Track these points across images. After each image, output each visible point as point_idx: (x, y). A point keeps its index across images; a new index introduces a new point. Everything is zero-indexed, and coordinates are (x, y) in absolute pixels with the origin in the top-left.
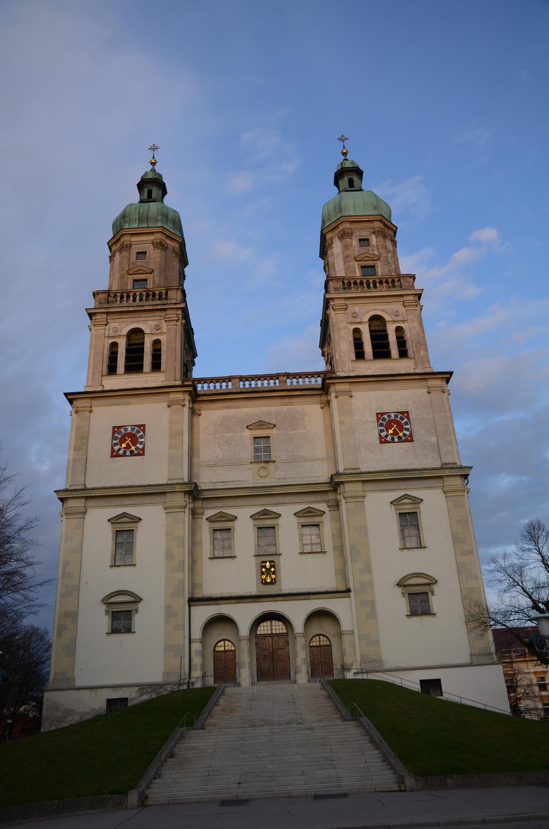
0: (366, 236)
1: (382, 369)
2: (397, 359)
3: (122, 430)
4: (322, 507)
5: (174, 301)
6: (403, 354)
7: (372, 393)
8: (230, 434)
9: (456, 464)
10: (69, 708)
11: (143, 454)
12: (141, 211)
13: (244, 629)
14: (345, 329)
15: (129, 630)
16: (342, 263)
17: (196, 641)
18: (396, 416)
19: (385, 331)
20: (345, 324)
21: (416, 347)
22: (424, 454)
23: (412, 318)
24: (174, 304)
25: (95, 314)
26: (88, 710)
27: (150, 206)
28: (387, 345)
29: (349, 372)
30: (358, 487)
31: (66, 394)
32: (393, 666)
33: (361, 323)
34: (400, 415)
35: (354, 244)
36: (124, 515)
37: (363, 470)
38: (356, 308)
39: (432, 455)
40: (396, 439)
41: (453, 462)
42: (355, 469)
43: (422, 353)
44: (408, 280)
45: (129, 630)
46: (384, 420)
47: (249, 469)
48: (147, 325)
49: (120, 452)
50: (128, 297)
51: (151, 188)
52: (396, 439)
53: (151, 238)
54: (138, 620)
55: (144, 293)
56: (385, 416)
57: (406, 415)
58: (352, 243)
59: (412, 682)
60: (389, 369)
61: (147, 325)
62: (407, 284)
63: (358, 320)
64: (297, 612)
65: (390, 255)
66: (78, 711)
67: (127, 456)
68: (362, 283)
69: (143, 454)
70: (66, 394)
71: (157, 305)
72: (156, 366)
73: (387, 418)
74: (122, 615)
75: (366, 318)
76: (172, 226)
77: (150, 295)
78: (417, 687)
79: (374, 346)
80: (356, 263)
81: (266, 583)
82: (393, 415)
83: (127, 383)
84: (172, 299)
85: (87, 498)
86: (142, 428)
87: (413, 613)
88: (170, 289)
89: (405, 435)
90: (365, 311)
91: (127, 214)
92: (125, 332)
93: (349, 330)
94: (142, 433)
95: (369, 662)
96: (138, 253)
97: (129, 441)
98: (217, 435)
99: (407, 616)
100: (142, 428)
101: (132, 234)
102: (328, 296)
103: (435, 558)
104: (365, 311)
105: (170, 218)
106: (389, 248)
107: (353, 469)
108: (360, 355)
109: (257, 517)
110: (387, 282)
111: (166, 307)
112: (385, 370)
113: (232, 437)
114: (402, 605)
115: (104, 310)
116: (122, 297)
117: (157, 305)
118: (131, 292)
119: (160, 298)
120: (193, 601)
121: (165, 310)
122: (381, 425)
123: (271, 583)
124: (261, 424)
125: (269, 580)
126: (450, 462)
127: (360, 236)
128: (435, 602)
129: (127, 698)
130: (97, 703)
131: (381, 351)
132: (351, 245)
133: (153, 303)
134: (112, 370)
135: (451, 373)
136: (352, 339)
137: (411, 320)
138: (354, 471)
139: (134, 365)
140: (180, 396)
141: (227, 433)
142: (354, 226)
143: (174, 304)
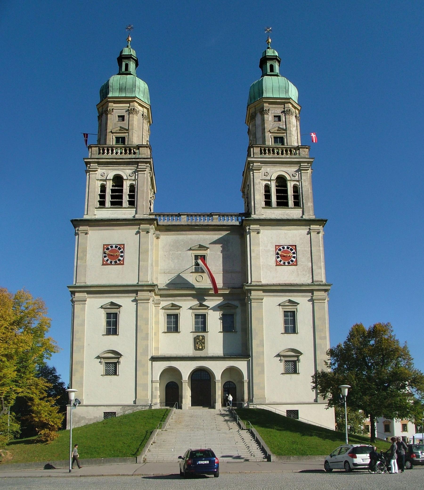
0: (279, 113)
1: (281, 214)
2: (292, 208)
3: (110, 247)
4: (236, 303)
5: (143, 156)
6: (297, 204)
7: (274, 231)
8: (179, 252)
9: (322, 281)
10: (82, 416)
11: (123, 264)
12: (121, 83)
13: (186, 376)
14: (260, 184)
15: (115, 373)
16: (261, 133)
17: (156, 382)
18: (288, 248)
19: (286, 186)
21: (306, 200)
22: (303, 274)
23: (305, 178)
24: (144, 159)
25: (90, 163)
26: (93, 418)
27: (128, 79)
28: (286, 198)
29: (260, 215)
30: (261, 293)
31: (72, 221)
32: (272, 401)
34: (290, 247)
35: (270, 120)
36: (112, 304)
37: (264, 282)
38: (268, 169)
39: (308, 275)
40: (286, 264)
41: (321, 280)
42: (259, 282)
44: (305, 150)
45: (115, 373)
47: (191, 276)
48: (126, 172)
49: (108, 262)
50: (112, 151)
51: (127, 62)
52: (286, 264)
53: (128, 105)
54: (120, 368)
55: (123, 149)
56: (281, 248)
57: (294, 247)
58: (268, 118)
59: (282, 411)
60: (286, 215)
61: (126, 172)
62: (304, 153)
63: (268, 178)
64: (218, 369)
65: (294, 129)
66: (87, 418)
67: (113, 265)
68: (273, 151)
69: (123, 264)
70: (72, 221)
71: (132, 159)
72: (132, 203)
73: (282, 249)
74: (111, 364)
75: (274, 177)
76: (142, 96)
77: (129, 150)
78: (284, 414)
79: (278, 197)
80: (270, 134)
81: (199, 349)
82: (286, 247)
83: (112, 214)
84: (142, 154)
85: (89, 293)
86: (122, 246)
87: (287, 372)
88: (141, 147)
89: (292, 261)
90: (275, 172)
93: (262, 185)
94: (122, 250)
95: (258, 399)
96: (119, 116)
97: (113, 255)
98: (171, 253)
99: (282, 374)
100: (122, 246)
101: (115, 102)
102: (249, 159)
103: (302, 340)
104: (275, 172)
106: (294, 124)
107: (257, 282)
108: (268, 204)
109: (195, 307)
110: (291, 151)
111: (138, 160)
112: (284, 215)
113: (180, 254)
114: (281, 366)
115: (96, 160)
116: (108, 150)
117: (132, 159)
118: (114, 147)
119: (135, 153)
120: (154, 359)
121: (137, 163)
123: (202, 349)
125: (200, 347)
126: (319, 280)
128: (301, 366)
129: (115, 412)
130: (98, 415)
131: (283, 202)
132: (268, 120)
133: (130, 156)
134: (102, 203)
135: (326, 221)
137: (304, 180)
138: (258, 284)
139: (117, 202)
140: (148, 226)
141: (177, 251)
142: (271, 106)
143: (144, 159)
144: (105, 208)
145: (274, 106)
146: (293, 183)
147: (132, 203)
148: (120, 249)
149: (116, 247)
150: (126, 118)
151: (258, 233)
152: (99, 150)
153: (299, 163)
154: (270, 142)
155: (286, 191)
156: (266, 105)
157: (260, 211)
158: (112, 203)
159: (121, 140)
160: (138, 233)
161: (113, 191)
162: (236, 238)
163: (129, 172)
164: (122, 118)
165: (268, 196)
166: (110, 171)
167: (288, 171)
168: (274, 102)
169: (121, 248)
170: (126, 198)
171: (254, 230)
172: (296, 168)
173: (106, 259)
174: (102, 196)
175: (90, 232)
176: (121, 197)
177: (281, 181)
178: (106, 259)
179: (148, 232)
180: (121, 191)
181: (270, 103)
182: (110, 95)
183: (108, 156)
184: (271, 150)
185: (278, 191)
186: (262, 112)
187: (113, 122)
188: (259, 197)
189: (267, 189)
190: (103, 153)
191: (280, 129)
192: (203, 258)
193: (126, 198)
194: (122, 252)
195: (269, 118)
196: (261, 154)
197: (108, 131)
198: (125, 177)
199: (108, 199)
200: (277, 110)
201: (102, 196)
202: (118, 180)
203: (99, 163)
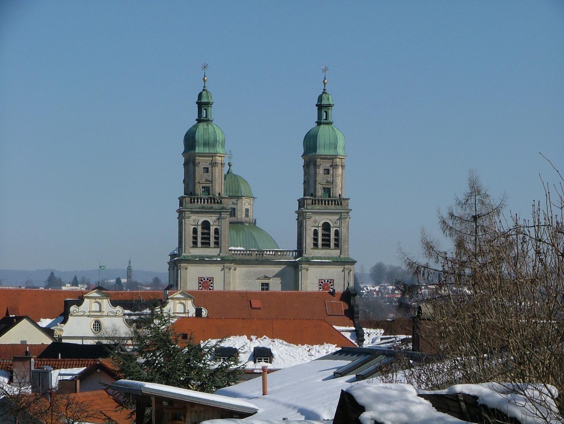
6: (337, 246)
20: (310, 227)
28: (329, 240)
33: (318, 227)
38: (317, 217)
43: (346, 246)
46: (322, 283)
48: (211, 219)
53: (211, 159)
61: (211, 219)
63: (317, 225)
75: (320, 225)
79: (323, 240)
91: (197, 140)
92: (200, 223)
101: (200, 156)
105: (220, 142)
108: (316, 245)
122: (320, 285)
124: (266, 277)
127: (324, 167)
136: (313, 236)
139: (206, 244)
144: (197, 247)
145: (325, 160)
146: (335, 229)
147: (217, 244)
148: (210, 281)
149: (208, 279)
150: (210, 170)
151: (307, 270)
152: (191, 199)
153: (341, 213)
154: (320, 192)
155: (329, 236)
156: (318, 160)
157: (310, 252)
158: (202, 243)
159: (207, 190)
160: (223, 269)
161: (202, 234)
162: (291, 270)
163: (214, 218)
164: (206, 170)
165: (316, 240)
166: (200, 218)
167: (331, 219)
168: (325, 158)
169: (211, 279)
170: (212, 240)
171: (305, 269)
172: (337, 217)
173: (201, 288)
174: (195, 238)
175: (189, 267)
176: (209, 239)
177: (326, 227)
178: (201, 288)
179: (230, 269)
180: (209, 234)
181: (321, 159)
182: (197, 151)
183: (197, 205)
184: (321, 201)
185: (323, 235)
186: (316, 166)
187: (199, 170)
188: (309, 240)
189: (316, 233)
190: (194, 202)
191: (328, 182)
192: (267, 284)
193: (212, 240)
194: (212, 283)
195: (320, 171)
196: (312, 204)
197: (197, 181)
198: (211, 223)
199: (199, 240)
200: (327, 164)
201: (195, 238)
202: (206, 225)
203: (192, 212)
